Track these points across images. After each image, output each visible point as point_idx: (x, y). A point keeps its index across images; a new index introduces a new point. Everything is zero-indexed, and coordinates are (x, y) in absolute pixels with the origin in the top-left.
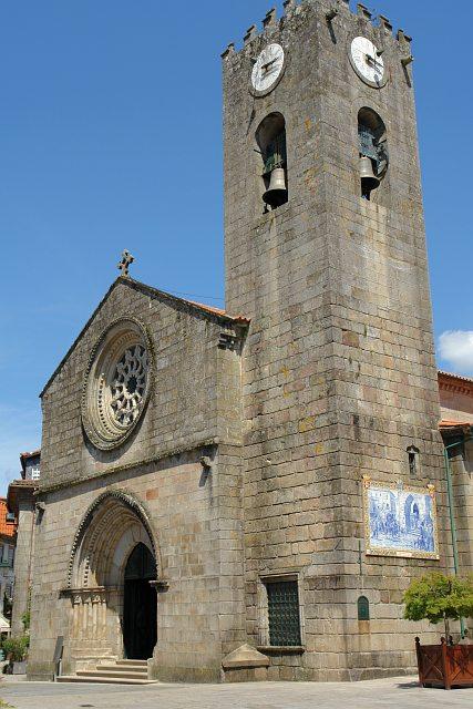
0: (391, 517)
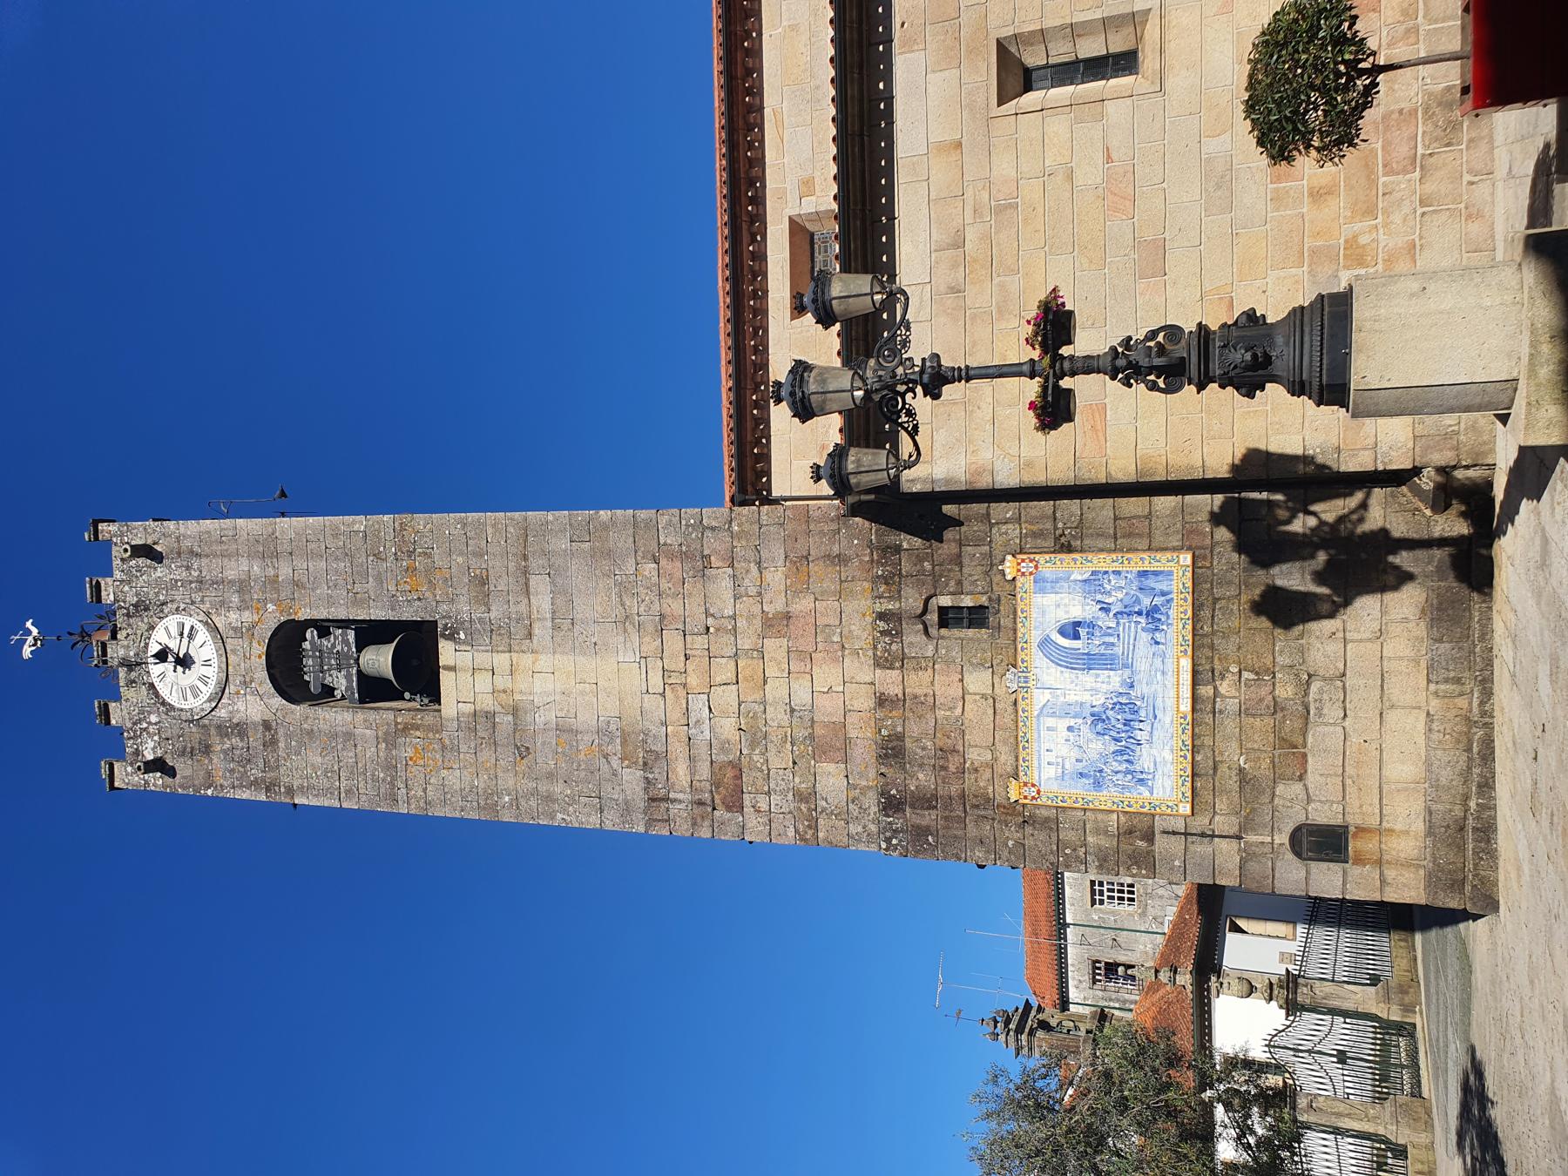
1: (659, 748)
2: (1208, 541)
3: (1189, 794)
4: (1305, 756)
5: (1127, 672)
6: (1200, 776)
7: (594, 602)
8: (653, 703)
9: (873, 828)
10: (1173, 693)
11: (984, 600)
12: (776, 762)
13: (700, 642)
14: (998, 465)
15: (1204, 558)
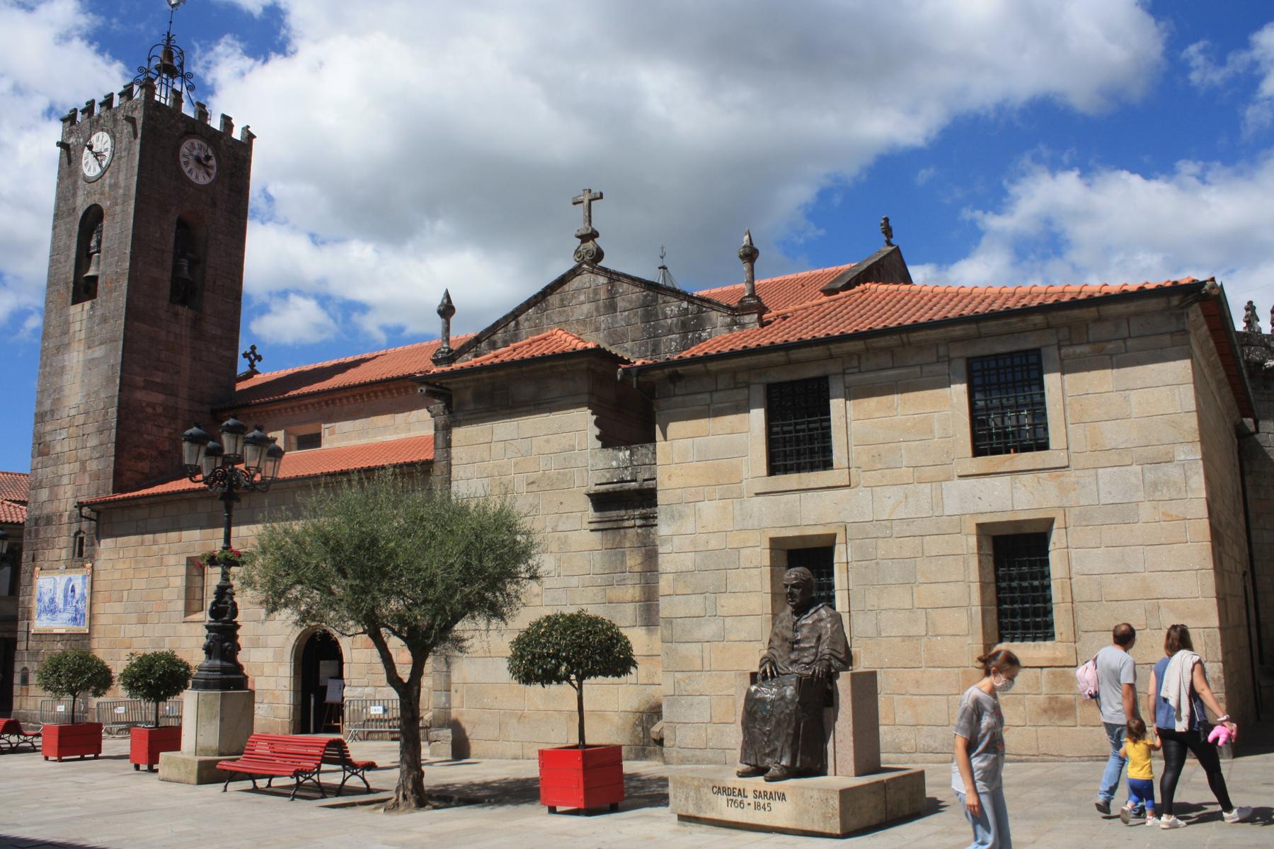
0: (52, 600)
6: (41, 636)
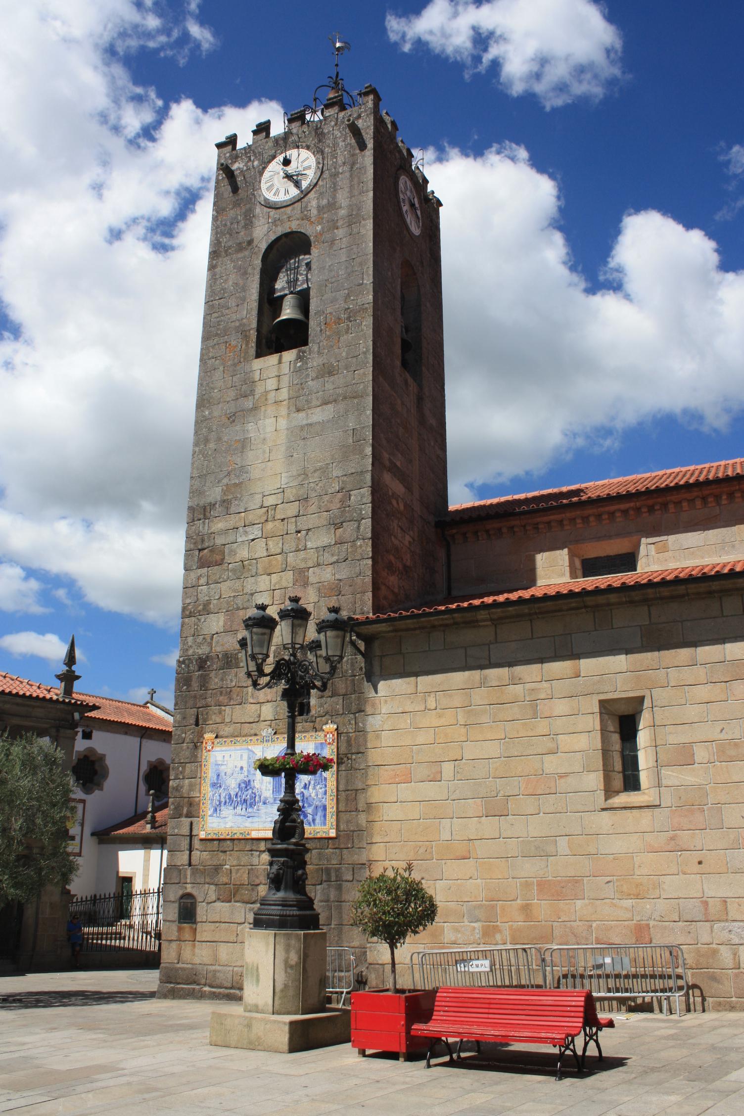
1: (233, 509)
2: (342, 846)
3: (210, 837)
4: (230, 901)
5: (271, 800)
6: (219, 843)
7: (318, 451)
8: (258, 498)
9: (190, 652)
10: (261, 826)
11: (313, 712)
12: (224, 586)
13: (292, 528)
14: (378, 717)
15: (334, 844)
